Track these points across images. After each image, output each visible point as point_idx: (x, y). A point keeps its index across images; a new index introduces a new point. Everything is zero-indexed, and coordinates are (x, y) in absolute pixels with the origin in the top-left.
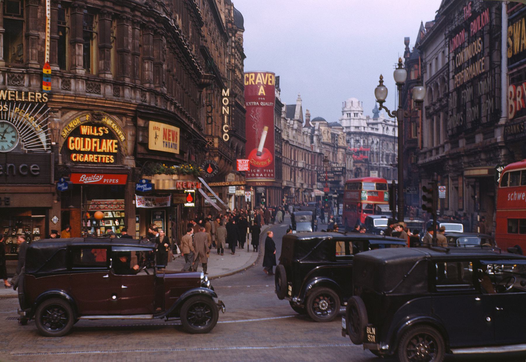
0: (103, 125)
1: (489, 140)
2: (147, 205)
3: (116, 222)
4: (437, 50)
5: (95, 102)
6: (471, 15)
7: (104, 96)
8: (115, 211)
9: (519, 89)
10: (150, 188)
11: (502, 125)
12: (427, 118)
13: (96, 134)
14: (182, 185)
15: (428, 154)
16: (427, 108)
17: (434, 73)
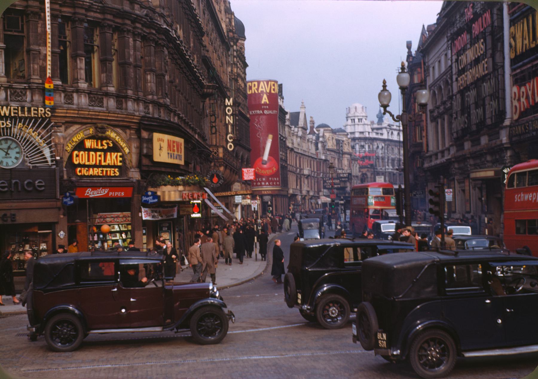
0: (107, 138)
1: (494, 141)
2: (153, 217)
3: (123, 235)
4: (440, 52)
5: (98, 115)
6: (472, 16)
7: (107, 109)
8: (122, 224)
9: (523, 89)
10: (156, 200)
11: (506, 126)
12: (432, 121)
13: (100, 147)
14: (188, 196)
15: (433, 158)
16: (431, 112)
17: (437, 76)
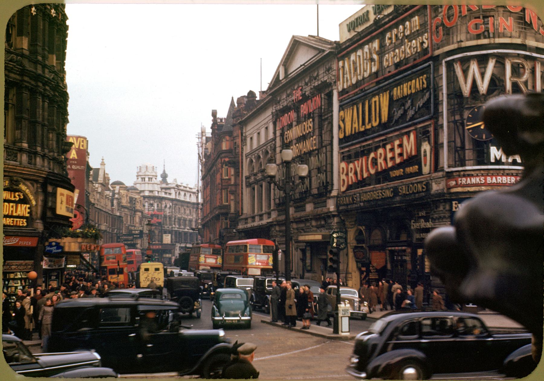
0: (19, 191)
1: (320, 209)
2: (49, 266)
3: (23, 282)
4: (260, 125)
5: (15, 169)
6: (301, 98)
7: (21, 163)
8: (23, 272)
9: (351, 165)
10: (60, 250)
11: (334, 197)
12: (247, 186)
13: (13, 199)
14: (86, 247)
15: (250, 220)
16: (247, 178)
17: (255, 146)
